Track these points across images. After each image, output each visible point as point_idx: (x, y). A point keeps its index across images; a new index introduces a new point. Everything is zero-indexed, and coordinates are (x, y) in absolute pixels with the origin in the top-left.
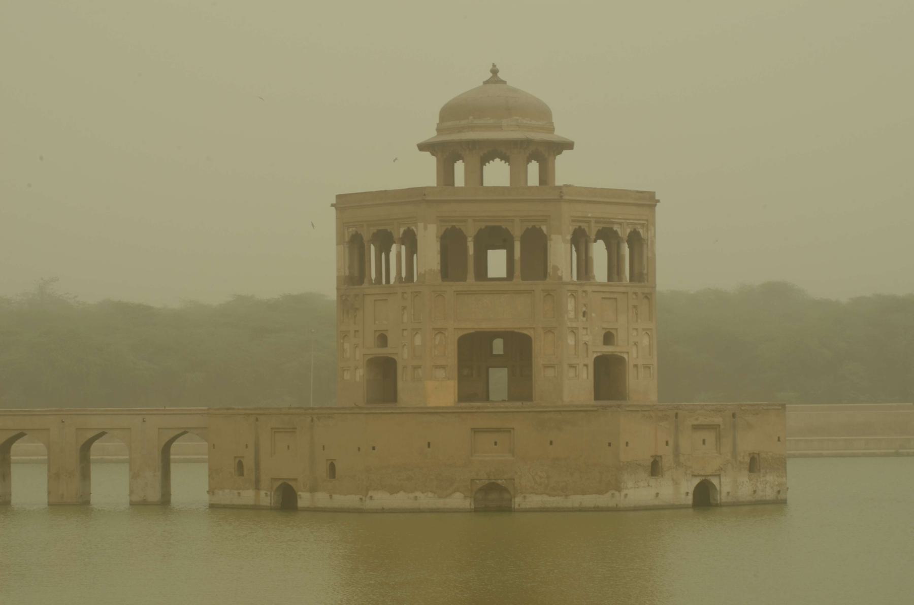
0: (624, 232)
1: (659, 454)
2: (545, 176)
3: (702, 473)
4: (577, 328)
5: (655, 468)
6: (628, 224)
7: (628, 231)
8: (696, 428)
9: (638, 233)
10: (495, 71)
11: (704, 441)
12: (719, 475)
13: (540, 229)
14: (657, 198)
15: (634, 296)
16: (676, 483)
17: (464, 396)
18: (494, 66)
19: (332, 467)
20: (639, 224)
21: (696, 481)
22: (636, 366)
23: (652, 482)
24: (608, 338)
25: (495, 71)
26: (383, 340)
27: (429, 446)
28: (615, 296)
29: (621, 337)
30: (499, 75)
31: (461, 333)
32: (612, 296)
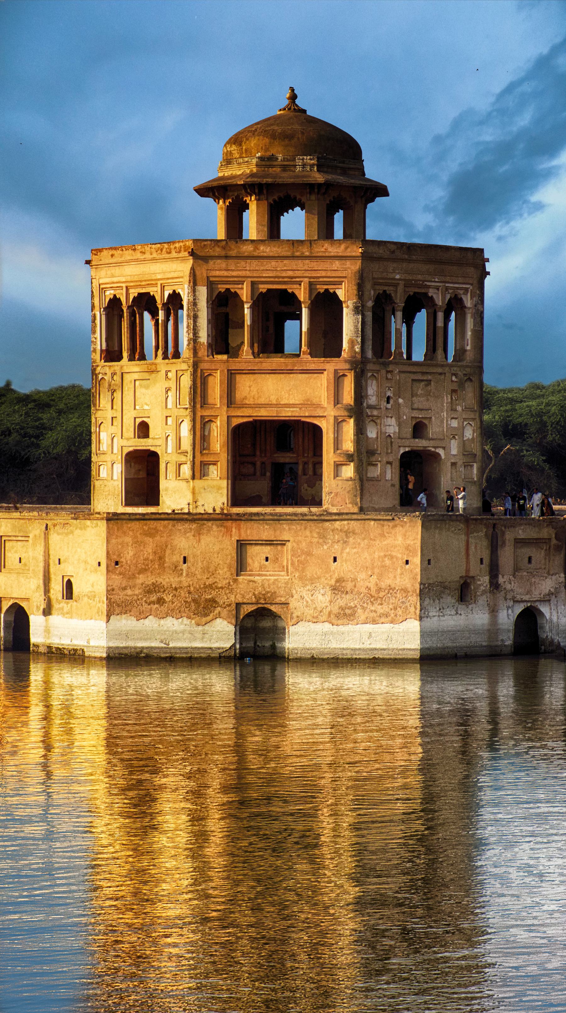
0: (440, 300)
1: (471, 574)
2: (355, 230)
3: (526, 598)
4: (378, 417)
5: (464, 592)
6: (447, 289)
7: (448, 297)
8: (519, 543)
9: (461, 300)
10: (293, 97)
11: (530, 559)
12: (549, 601)
13: (335, 295)
14: (486, 257)
15: (454, 378)
16: (493, 611)
17: (237, 499)
19: (69, 585)
20: (461, 289)
21: (519, 609)
22: (454, 464)
23: (462, 608)
24: (419, 429)
25: (293, 97)
26: (143, 430)
27: (185, 562)
28: (430, 377)
30: (297, 101)
31: (236, 422)
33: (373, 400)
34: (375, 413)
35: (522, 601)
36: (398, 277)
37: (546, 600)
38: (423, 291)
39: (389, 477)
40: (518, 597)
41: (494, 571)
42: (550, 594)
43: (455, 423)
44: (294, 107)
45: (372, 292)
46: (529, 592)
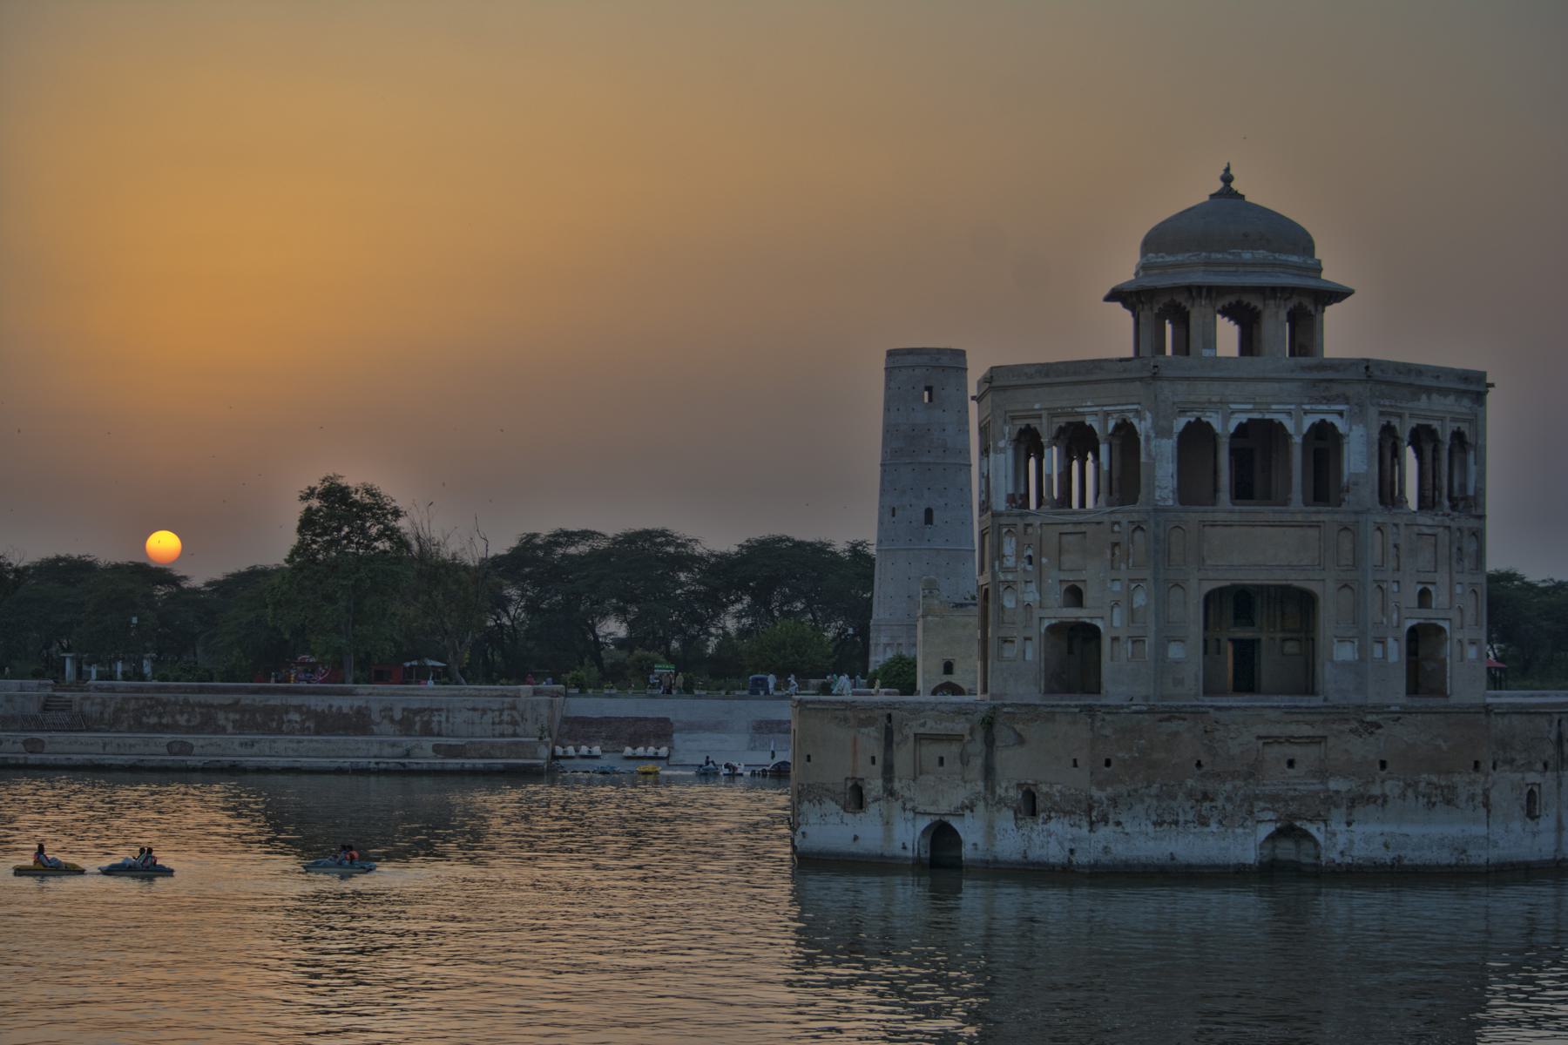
3: (931, 809)
5: (856, 799)
6: (1107, 414)
7: (1111, 424)
8: (919, 738)
9: (1132, 425)
10: (1227, 178)
15: (1116, 528)
18: (1227, 170)
21: (924, 823)
22: (1115, 639)
23: (848, 817)
24: (1075, 595)
25: (1227, 178)
28: (1083, 528)
29: (1089, 596)
32: (1078, 529)
33: (1010, 562)
34: (1010, 577)
35: (925, 813)
36: (1037, 406)
37: (958, 813)
38: (1079, 419)
39: (1029, 657)
40: (921, 809)
41: (888, 771)
42: (964, 807)
43: (1117, 587)
44: (1227, 193)
45: (1007, 429)
46: (934, 803)
